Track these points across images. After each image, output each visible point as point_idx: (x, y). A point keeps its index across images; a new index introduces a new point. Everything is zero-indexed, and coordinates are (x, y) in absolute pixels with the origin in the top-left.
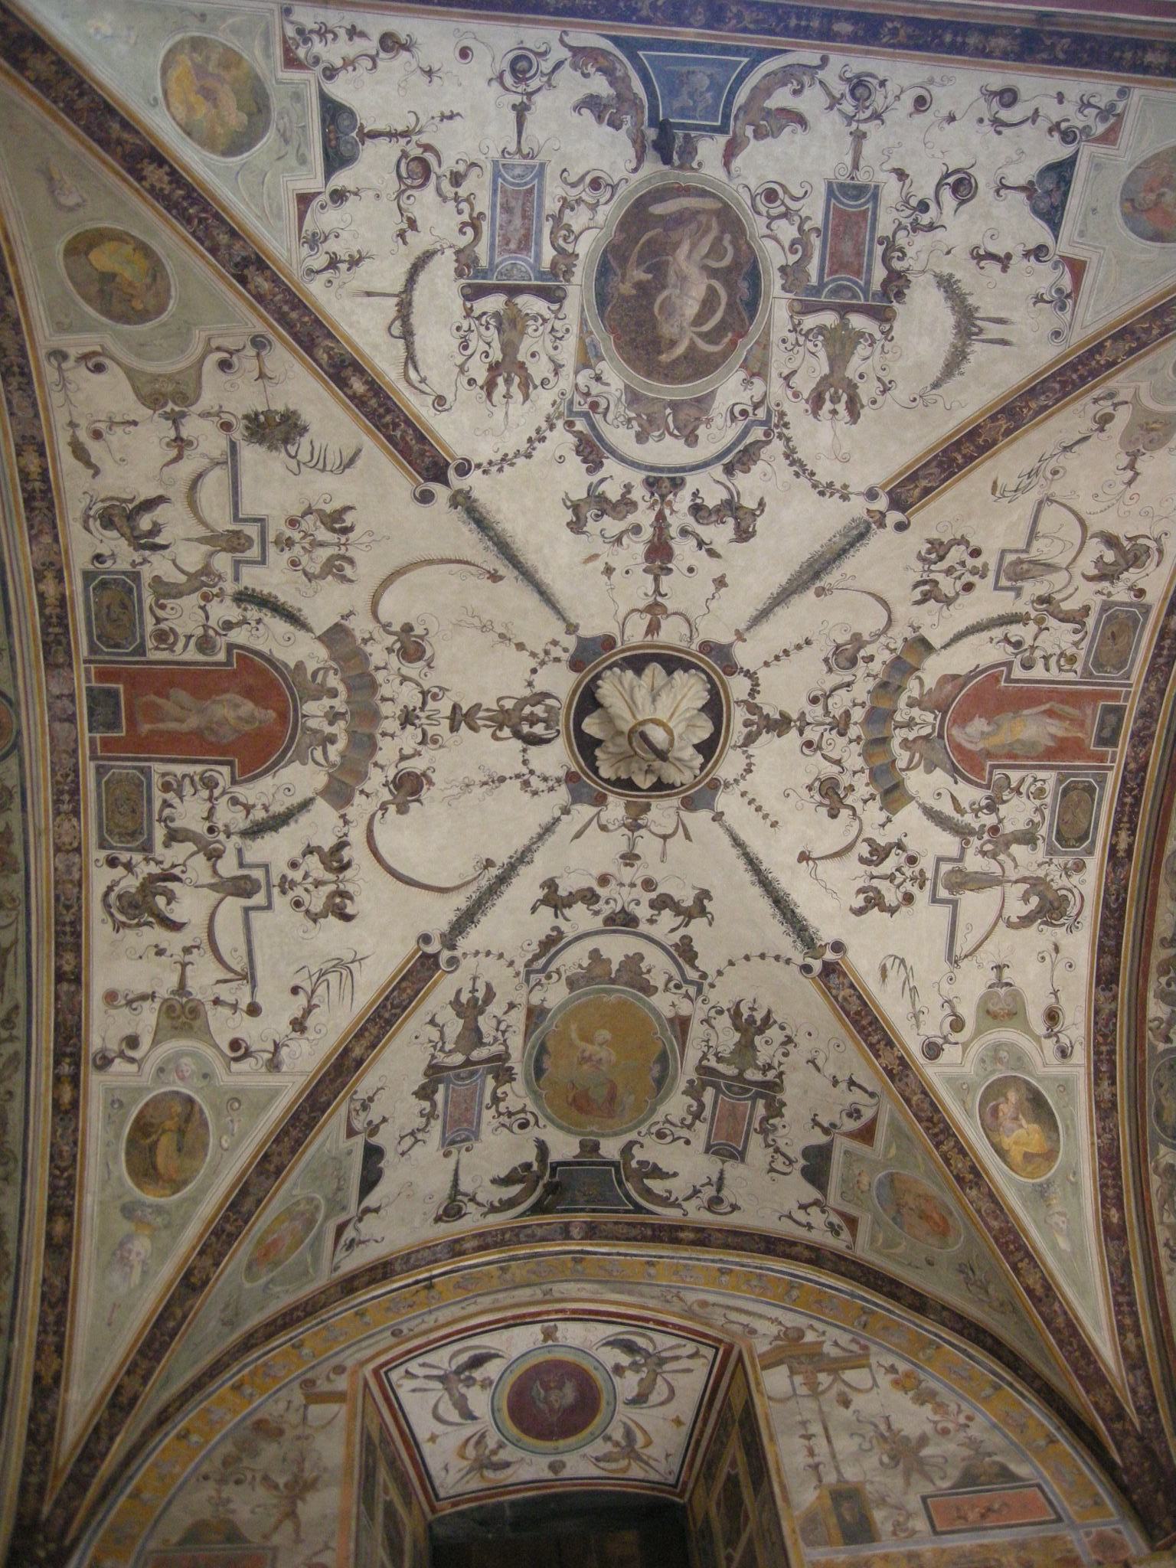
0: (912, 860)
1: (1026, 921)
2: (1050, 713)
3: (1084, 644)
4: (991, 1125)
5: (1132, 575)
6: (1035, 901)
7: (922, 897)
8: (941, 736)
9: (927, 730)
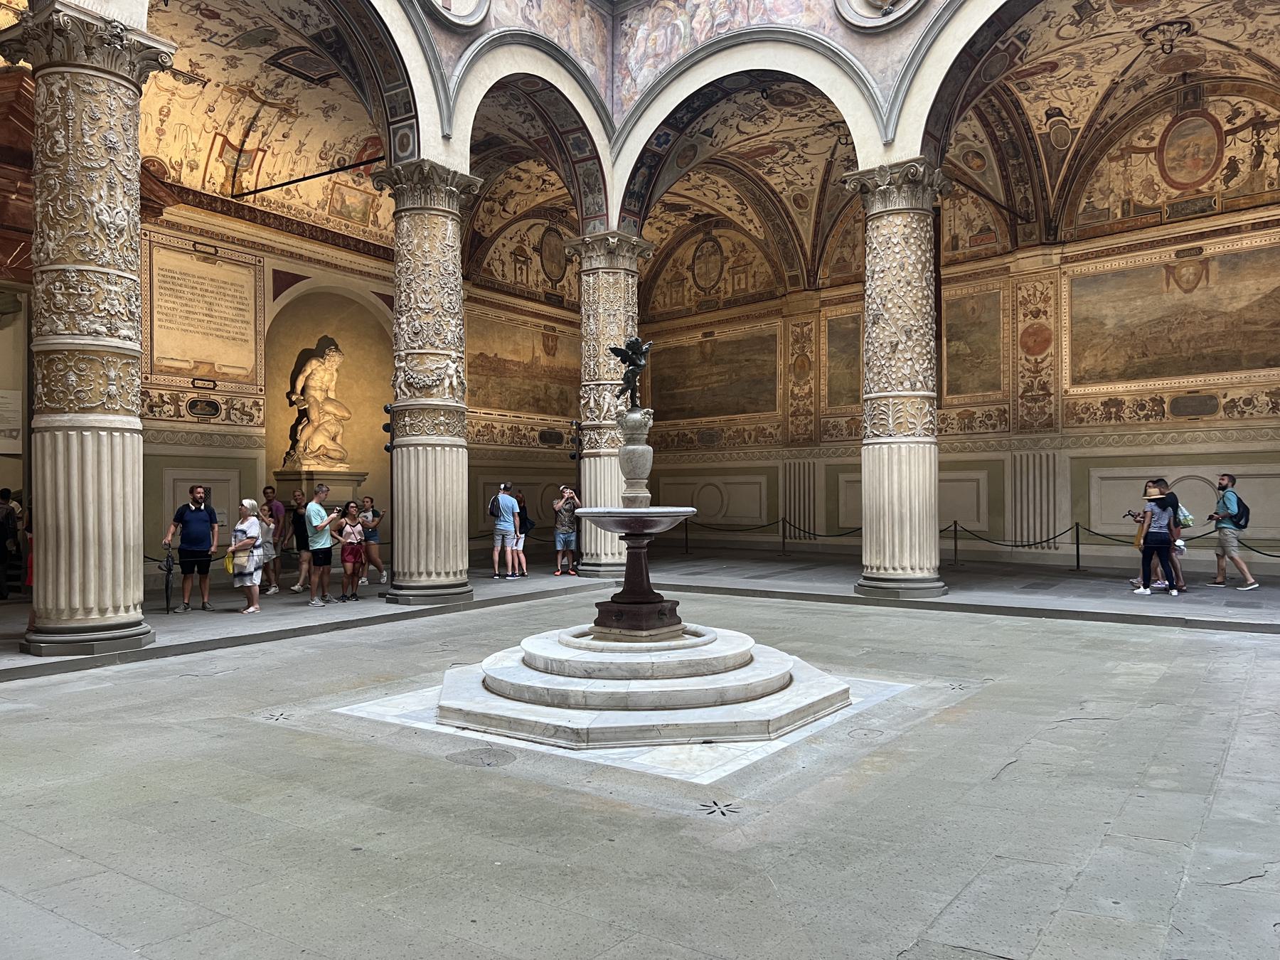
4: (967, 163)
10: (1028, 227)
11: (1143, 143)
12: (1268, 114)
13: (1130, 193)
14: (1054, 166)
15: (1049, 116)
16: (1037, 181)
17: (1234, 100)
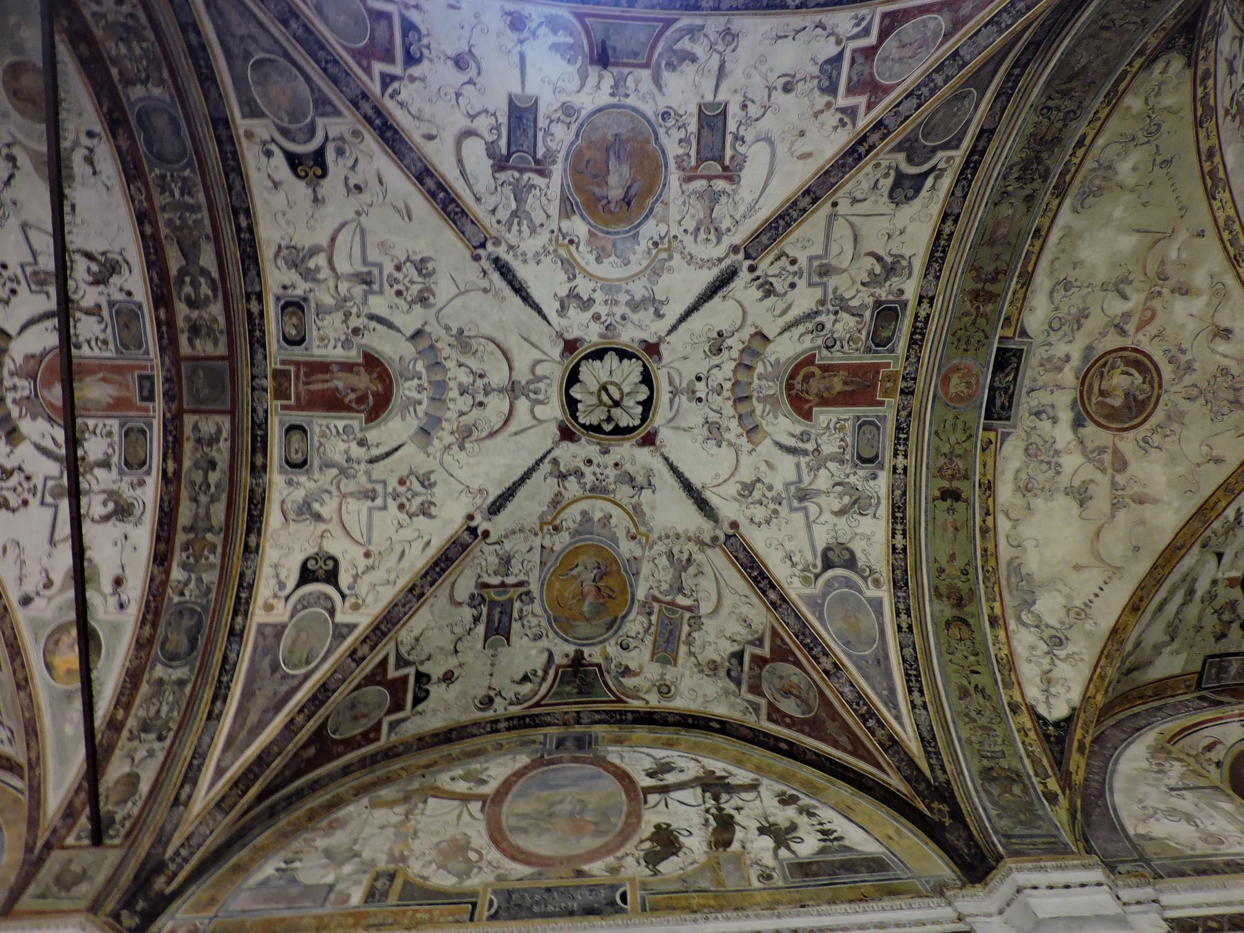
0: (28, 478)
1: (105, 518)
2: (105, 380)
3: (109, 330)
5: (114, 280)
6: (111, 506)
7: (34, 502)
8: (36, 395)
9: (26, 393)
10: (87, 857)
11: (462, 787)
12: (731, 774)
13: (403, 859)
14: (253, 718)
15: (306, 575)
16: (188, 752)
17: (660, 753)
